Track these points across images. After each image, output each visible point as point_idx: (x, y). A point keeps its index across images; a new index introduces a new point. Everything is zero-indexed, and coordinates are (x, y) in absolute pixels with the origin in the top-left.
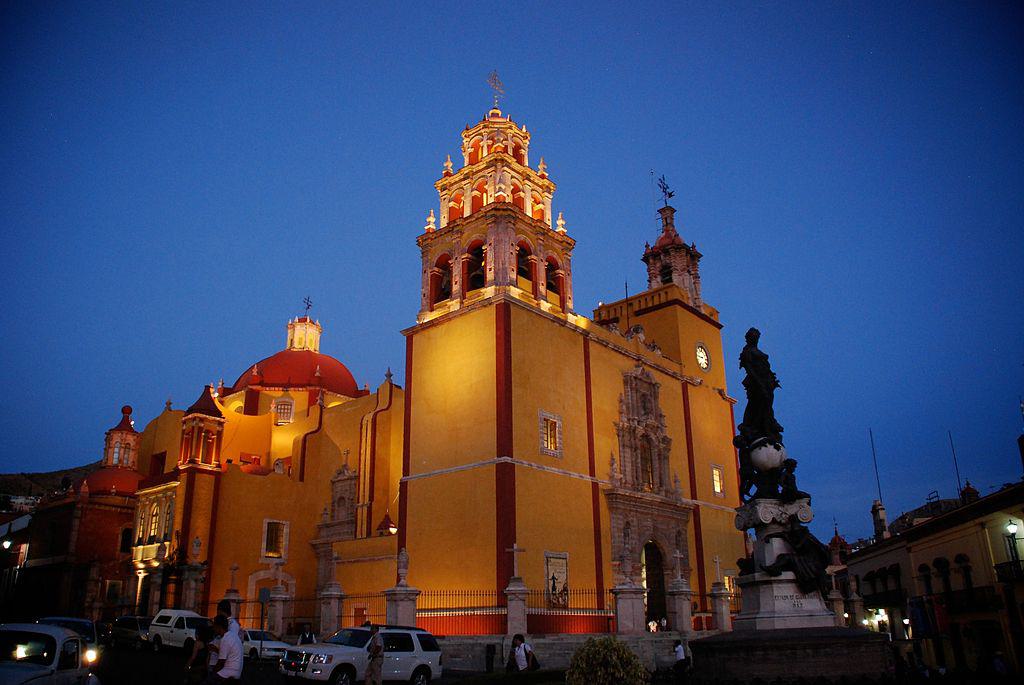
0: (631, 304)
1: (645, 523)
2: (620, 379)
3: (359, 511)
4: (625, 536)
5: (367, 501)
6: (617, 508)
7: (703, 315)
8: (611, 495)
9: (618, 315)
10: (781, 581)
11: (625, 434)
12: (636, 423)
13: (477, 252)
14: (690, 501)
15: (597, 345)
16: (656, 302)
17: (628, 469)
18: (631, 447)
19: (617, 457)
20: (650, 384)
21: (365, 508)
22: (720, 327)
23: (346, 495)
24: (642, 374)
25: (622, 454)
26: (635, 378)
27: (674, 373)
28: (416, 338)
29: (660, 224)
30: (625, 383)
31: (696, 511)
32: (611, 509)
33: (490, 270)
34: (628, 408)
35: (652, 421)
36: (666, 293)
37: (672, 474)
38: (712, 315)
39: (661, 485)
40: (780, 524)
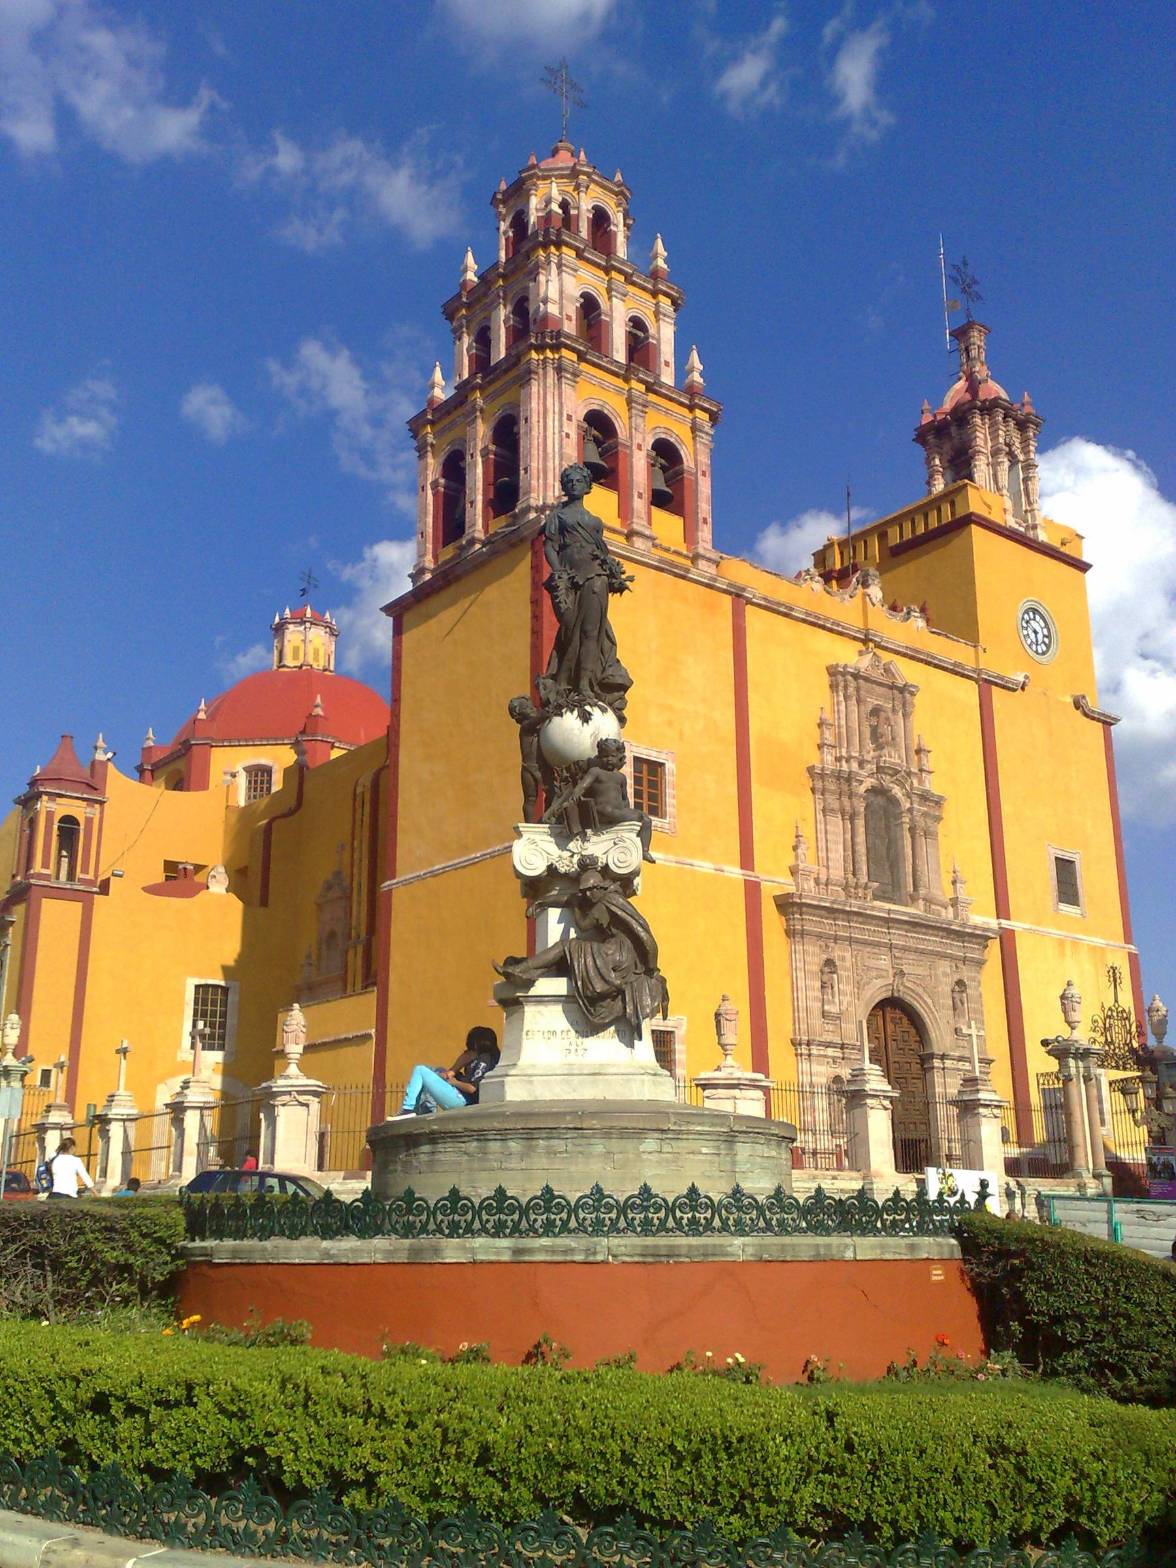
0: (883, 536)
1: (872, 963)
2: (826, 680)
3: (351, 952)
4: (822, 987)
5: (363, 935)
6: (803, 933)
7: (1042, 544)
8: (785, 904)
10: (541, 1000)
12: (855, 766)
14: (993, 923)
16: (933, 523)
17: (838, 854)
19: (808, 832)
20: (892, 687)
21: (360, 950)
22: (1083, 567)
25: (821, 827)
26: (856, 676)
27: (956, 664)
30: (833, 687)
31: (1007, 939)
35: (892, 757)
36: (953, 504)
37: (946, 865)
38: (1063, 544)
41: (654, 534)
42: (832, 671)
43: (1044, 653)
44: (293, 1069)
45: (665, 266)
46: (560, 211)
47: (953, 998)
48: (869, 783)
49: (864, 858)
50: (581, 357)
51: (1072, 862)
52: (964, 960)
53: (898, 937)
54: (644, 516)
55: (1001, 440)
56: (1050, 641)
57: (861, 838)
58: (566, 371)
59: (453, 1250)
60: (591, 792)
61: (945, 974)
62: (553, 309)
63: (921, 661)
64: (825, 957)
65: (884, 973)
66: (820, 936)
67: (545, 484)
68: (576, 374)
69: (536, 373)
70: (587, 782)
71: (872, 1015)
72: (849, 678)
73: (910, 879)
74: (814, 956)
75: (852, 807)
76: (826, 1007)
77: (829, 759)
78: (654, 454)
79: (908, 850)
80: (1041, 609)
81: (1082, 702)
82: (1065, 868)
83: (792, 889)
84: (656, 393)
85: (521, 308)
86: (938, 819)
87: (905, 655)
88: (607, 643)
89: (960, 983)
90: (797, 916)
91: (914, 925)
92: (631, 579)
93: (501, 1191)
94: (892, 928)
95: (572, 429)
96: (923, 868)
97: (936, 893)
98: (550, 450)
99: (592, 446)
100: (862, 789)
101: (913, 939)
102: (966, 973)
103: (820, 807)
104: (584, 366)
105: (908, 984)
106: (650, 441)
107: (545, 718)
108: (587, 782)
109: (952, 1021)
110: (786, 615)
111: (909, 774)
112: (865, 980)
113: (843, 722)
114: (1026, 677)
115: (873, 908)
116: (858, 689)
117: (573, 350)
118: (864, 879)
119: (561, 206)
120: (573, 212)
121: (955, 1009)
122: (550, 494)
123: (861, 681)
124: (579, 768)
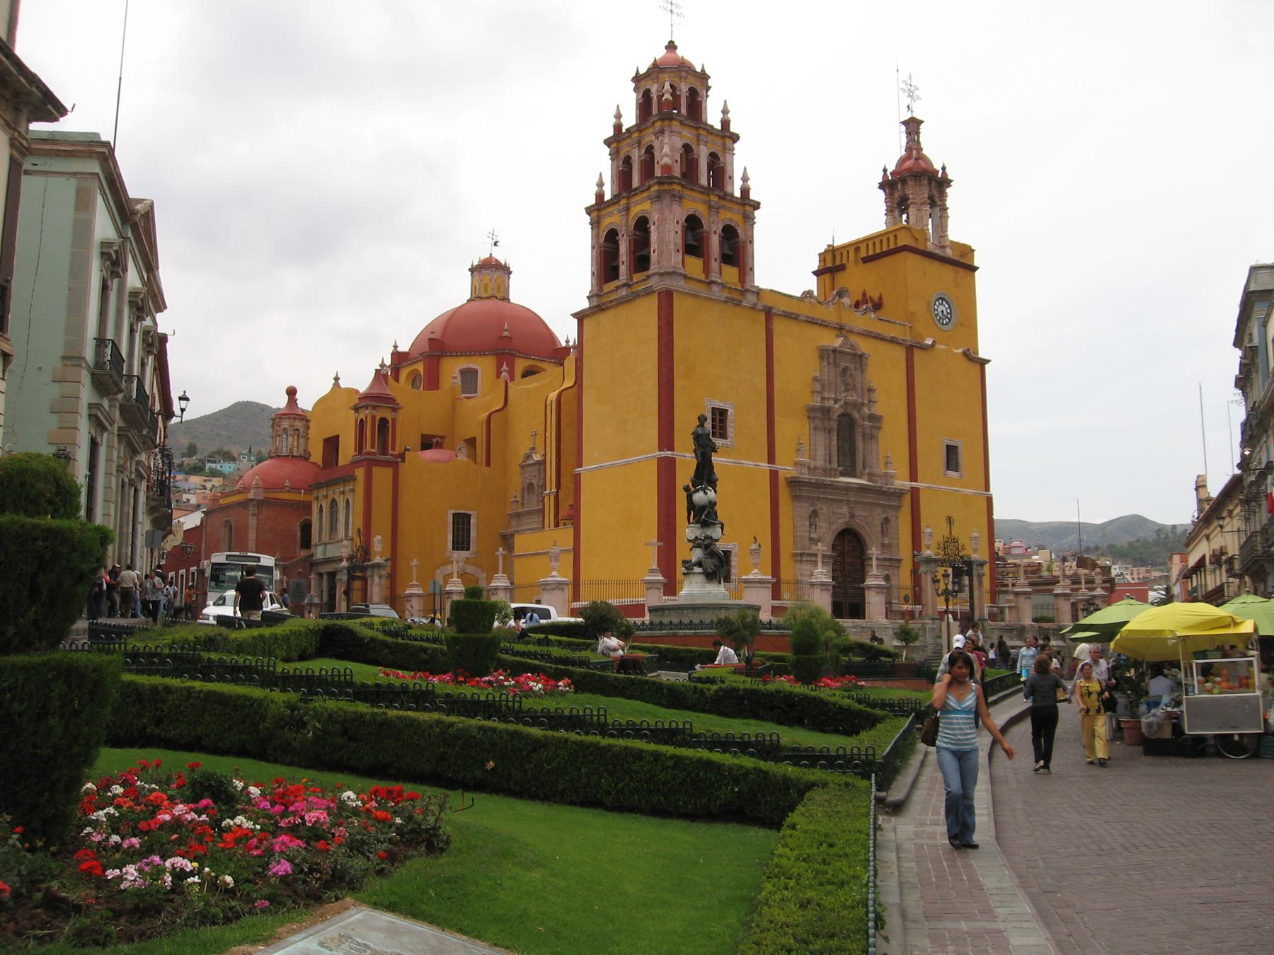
0: (857, 249)
1: (836, 511)
2: (816, 355)
3: (547, 499)
4: (810, 525)
5: (554, 490)
9: (844, 261)
10: (694, 573)
11: (818, 414)
12: (832, 402)
13: (642, 224)
15: (786, 321)
17: (821, 452)
18: (825, 429)
20: (855, 355)
22: (977, 268)
23: (535, 482)
24: (843, 344)
26: (834, 351)
27: (893, 337)
28: (586, 322)
29: (904, 139)
30: (821, 357)
31: (915, 492)
32: (796, 498)
33: (654, 252)
34: (823, 386)
35: (853, 397)
36: (896, 236)
39: (864, 467)
40: (700, 539)
43: (947, 324)
47: (882, 528)
48: (839, 412)
50: (683, 186)
51: (956, 447)
52: (890, 507)
54: (717, 271)
55: (926, 196)
57: (834, 443)
59: (681, 632)
61: (879, 514)
62: (666, 160)
64: (812, 509)
66: (809, 498)
68: (681, 198)
70: (706, 512)
72: (830, 352)
73: (861, 464)
74: (806, 509)
76: (812, 535)
77: (819, 399)
81: (968, 353)
82: (951, 451)
83: (795, 474)
84: (724, 199)
85: (650, 150)
86: (879, 428)
87: (863, 335)
89: (887, 520)
91: (861, 489)
93: (691, 622)
95: (679, 229)
97: (876, 470)
99: (690, 234)
100: (835, 416)
102: (890, 513)
103: (812, 426)
104: (686, 192)
105: (857, 521)
106: (721, 227)
108: (706, 512)
110: (796, 319)
111: (863, 404)
113: (826, 377)
114: (934, 341)
115: (838, 482)
116: (835, 359)
117: (679, 184)
118: (835, 465)
120: (678, 93)
121: (882, 531)
123: (838, 355)
124: (703, 508)
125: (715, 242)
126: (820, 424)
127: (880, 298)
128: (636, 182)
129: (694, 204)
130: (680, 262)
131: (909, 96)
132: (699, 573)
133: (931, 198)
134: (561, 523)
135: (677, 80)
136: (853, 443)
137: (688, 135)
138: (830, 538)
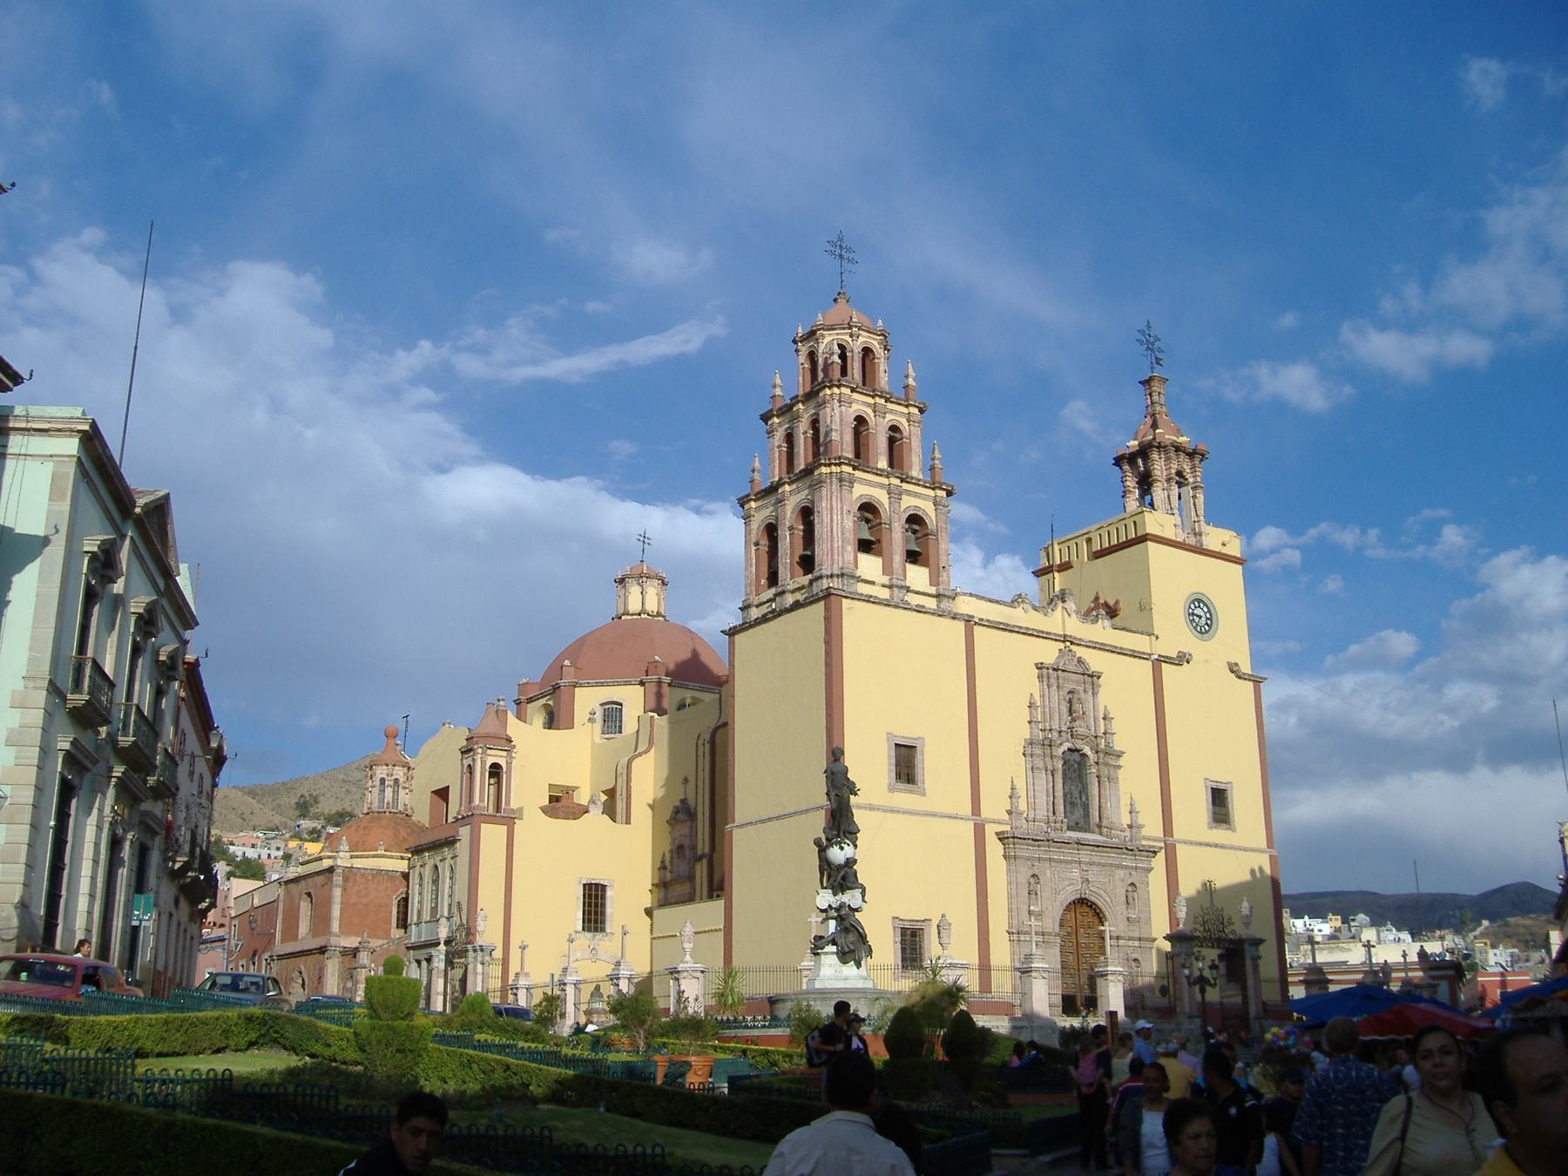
5: (707, 850)
6: (1015, 857)
10: (826, 953)
11: (1037, 747)
12: (1055, 734)
13: (807, 514)
17: (1043, 801)
18: (1046, 770)
30: (1040, 677)
41: (908, 585)
42: (1040, 666)
44: (688, 957)
45: (914, 384)
46: (840, 361)
47: (1127, 897)
49: (1062, 801)
53: (1085, 855)
54: (900, 572)
55: (1173, 471)
56: (1212, 623)
58: (845, 481)
60: (844, 878)
63: (1108, 651)
65: (1075, 882)
67: (832, 559)
68: (852, 482)
69: (825, 482)
71: (1068, 909)
72: (1050, 671)
75: (1053, 766)
76: (1032, 908)
78: (907, 526)
79: (1095, 792)
80: (1205, 599)
82: (1219, 797)
85: (815, 423)
86: (1119, 767)
88: (850, 815)
90: (1011, 846)
92: (859, 790)
94: (1081, 850)
95: (849, 523)
96: (1107, 805)
98: (835, 536)
100: (1061, 750)
101: (1096, 857)
104: (858, 474)
105: (1091, 888)
107: (827, 847)
109: (1125, 912)
112: (1061, 887)
119: (840, 357)
121: (1127, 903)
122: (835, 566)
124: (839, 867)
125: (897, 538)
126: (1039, 763)
127: (1117, 602)
128: (800, 465)
129: (868, 488)
130: (852, 562)
131: (1148, 348)
132: (833, 953)
133: (1179, 474)
134: (715, 894)
135: (847, 338)
136: (1084, 790)
137: (860, 404)
138: (1058, 911)
